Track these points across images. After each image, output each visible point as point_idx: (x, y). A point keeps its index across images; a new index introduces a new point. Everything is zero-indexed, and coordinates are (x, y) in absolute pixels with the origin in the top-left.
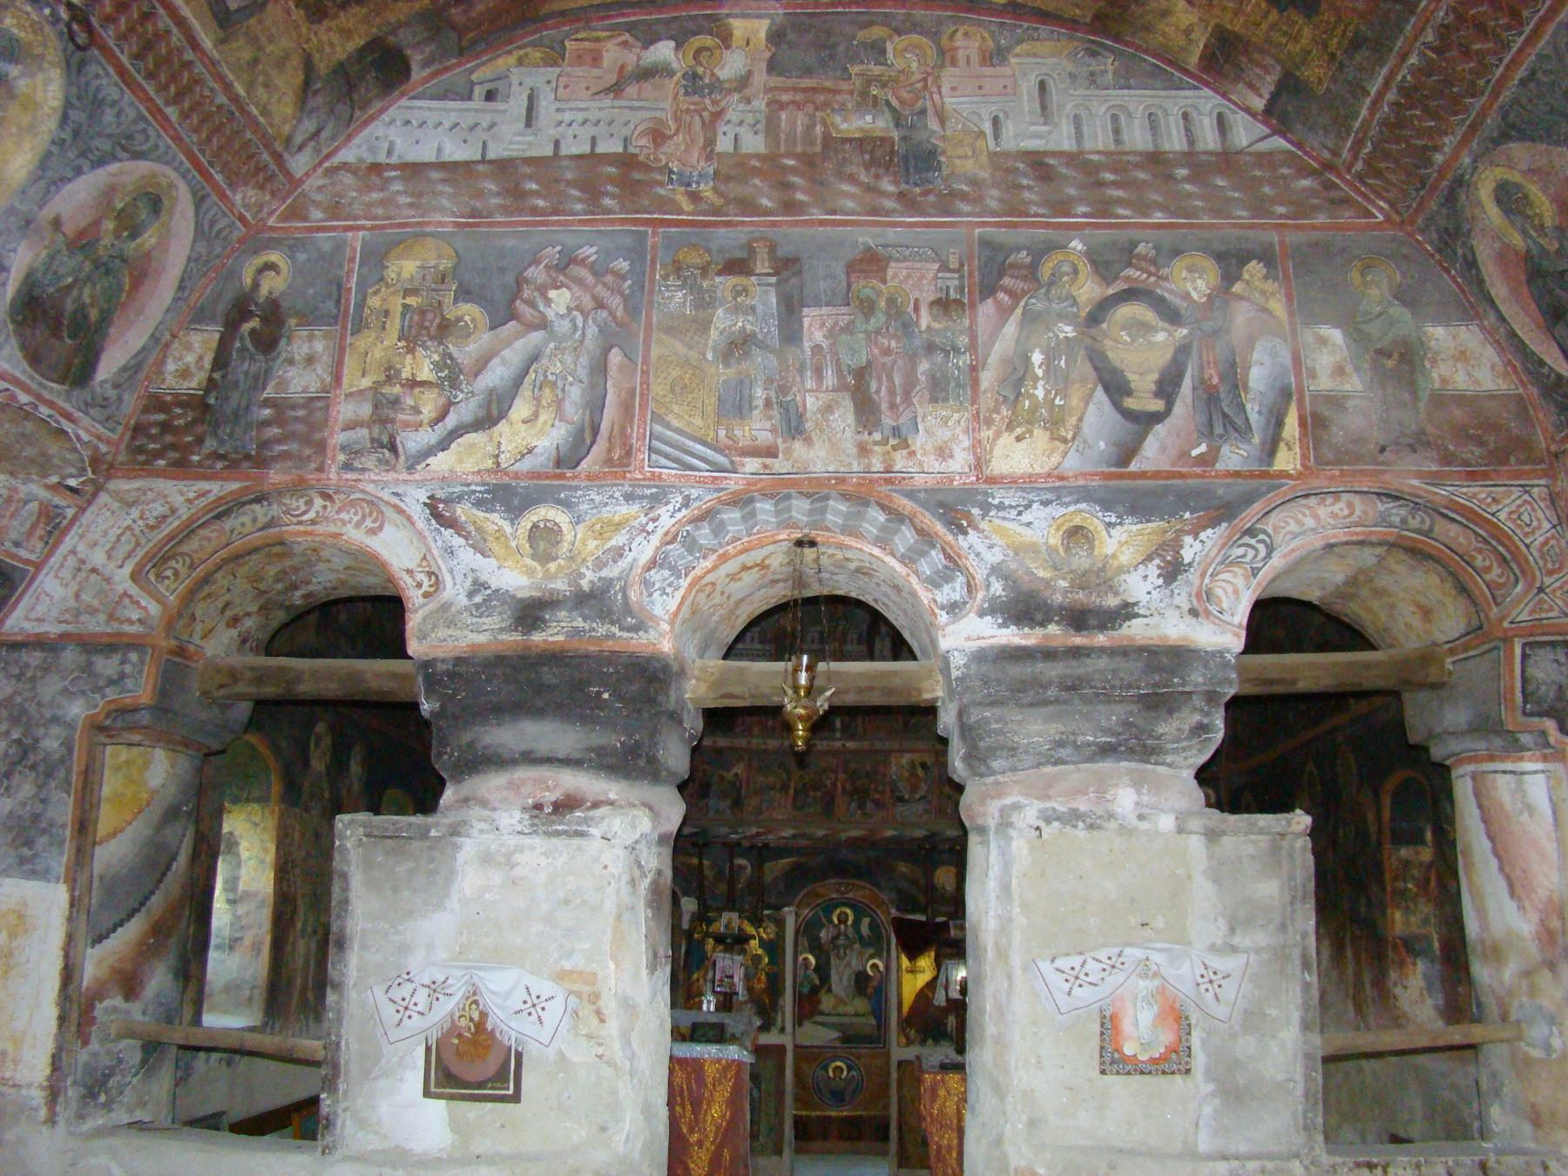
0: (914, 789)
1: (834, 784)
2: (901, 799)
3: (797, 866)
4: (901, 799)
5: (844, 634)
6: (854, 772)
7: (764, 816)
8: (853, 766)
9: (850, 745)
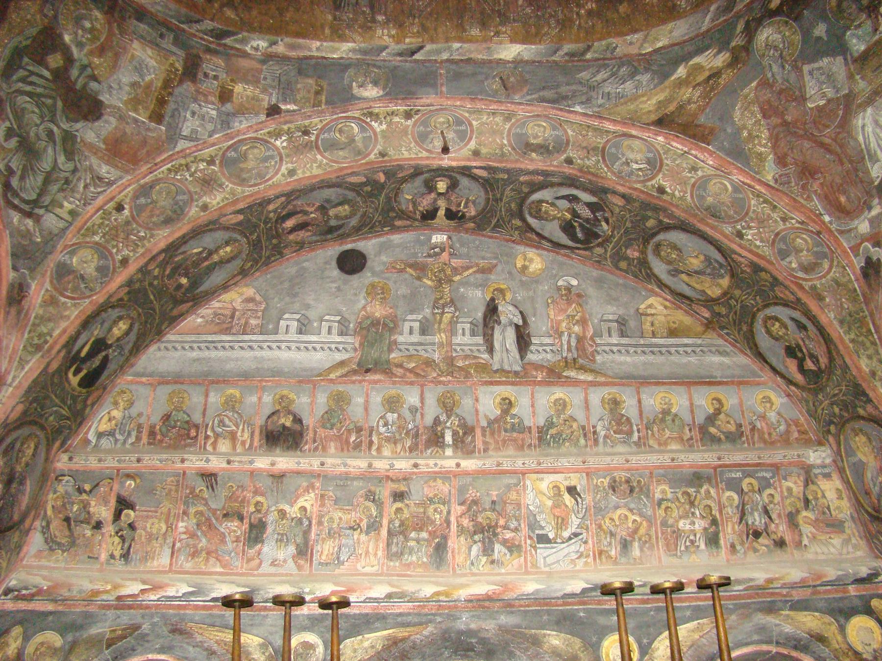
0: (562, 523)
1: (448, 523)
2: (543, 539)
3: (395, 642)
4: (543, 539)
5: (453, 323)
6: (475, 502)
7: (342, 569)
8: (471, 494)
9: (470, 464)
